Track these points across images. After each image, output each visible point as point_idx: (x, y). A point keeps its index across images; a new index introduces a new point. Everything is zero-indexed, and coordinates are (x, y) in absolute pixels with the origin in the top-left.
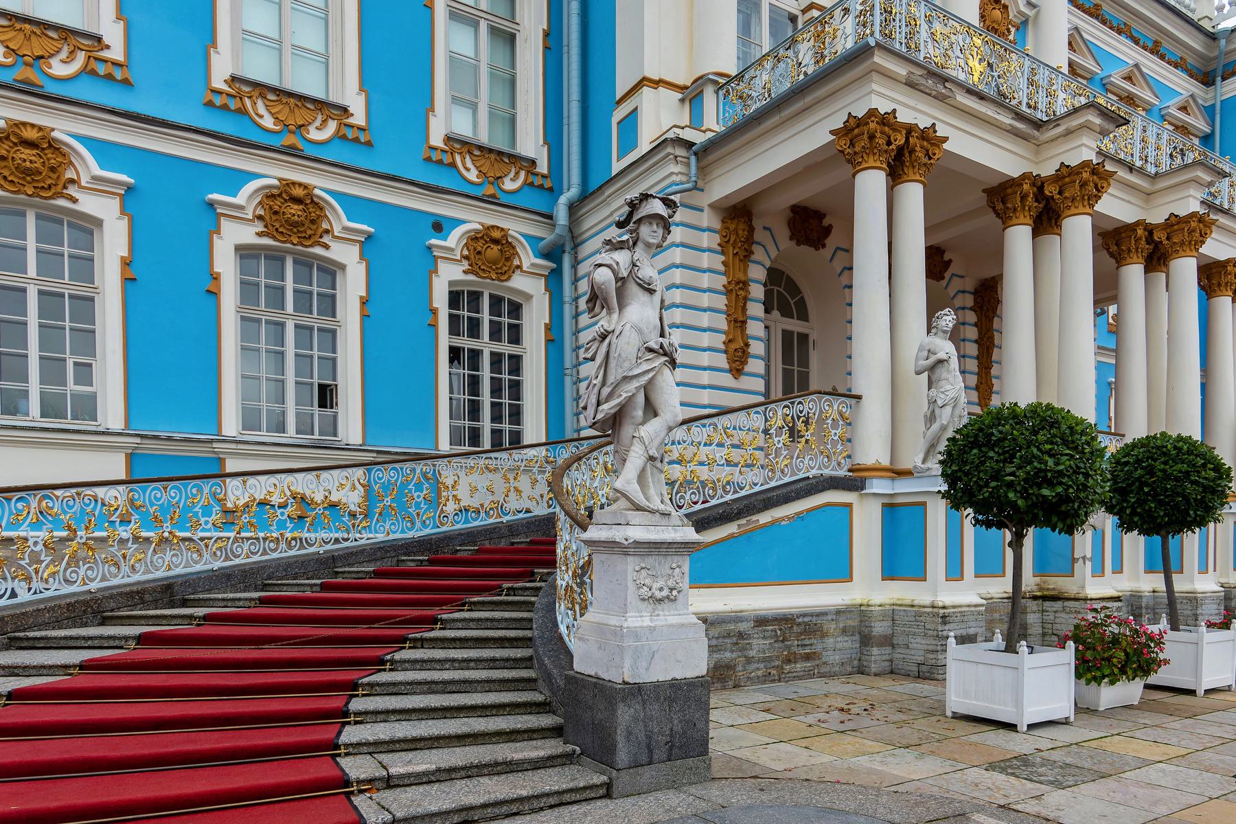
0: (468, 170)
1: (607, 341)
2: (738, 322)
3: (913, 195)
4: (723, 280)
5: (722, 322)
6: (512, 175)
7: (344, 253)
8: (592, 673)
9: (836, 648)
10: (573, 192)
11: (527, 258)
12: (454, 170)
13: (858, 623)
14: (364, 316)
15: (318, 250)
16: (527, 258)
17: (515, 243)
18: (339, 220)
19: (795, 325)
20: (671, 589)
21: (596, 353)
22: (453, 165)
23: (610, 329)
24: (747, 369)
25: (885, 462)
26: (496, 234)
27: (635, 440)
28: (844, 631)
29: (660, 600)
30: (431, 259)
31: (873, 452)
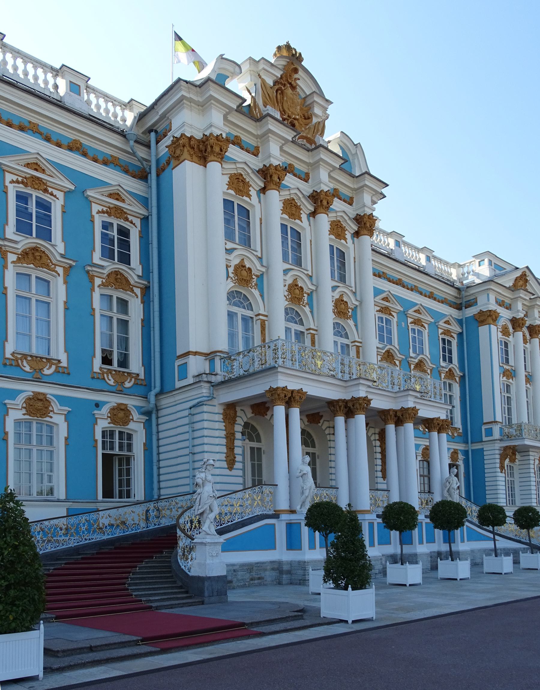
0: (110, 380)
2: (230, 448)
4: (224, 432)
5: (224, 449)
6: (128, 380)
10: (158, 389)
11: (135, 415)
16: (135, 415)
18: (56, 406)
19: (255, 445)
24: (235, 467)
31: (283, 505)
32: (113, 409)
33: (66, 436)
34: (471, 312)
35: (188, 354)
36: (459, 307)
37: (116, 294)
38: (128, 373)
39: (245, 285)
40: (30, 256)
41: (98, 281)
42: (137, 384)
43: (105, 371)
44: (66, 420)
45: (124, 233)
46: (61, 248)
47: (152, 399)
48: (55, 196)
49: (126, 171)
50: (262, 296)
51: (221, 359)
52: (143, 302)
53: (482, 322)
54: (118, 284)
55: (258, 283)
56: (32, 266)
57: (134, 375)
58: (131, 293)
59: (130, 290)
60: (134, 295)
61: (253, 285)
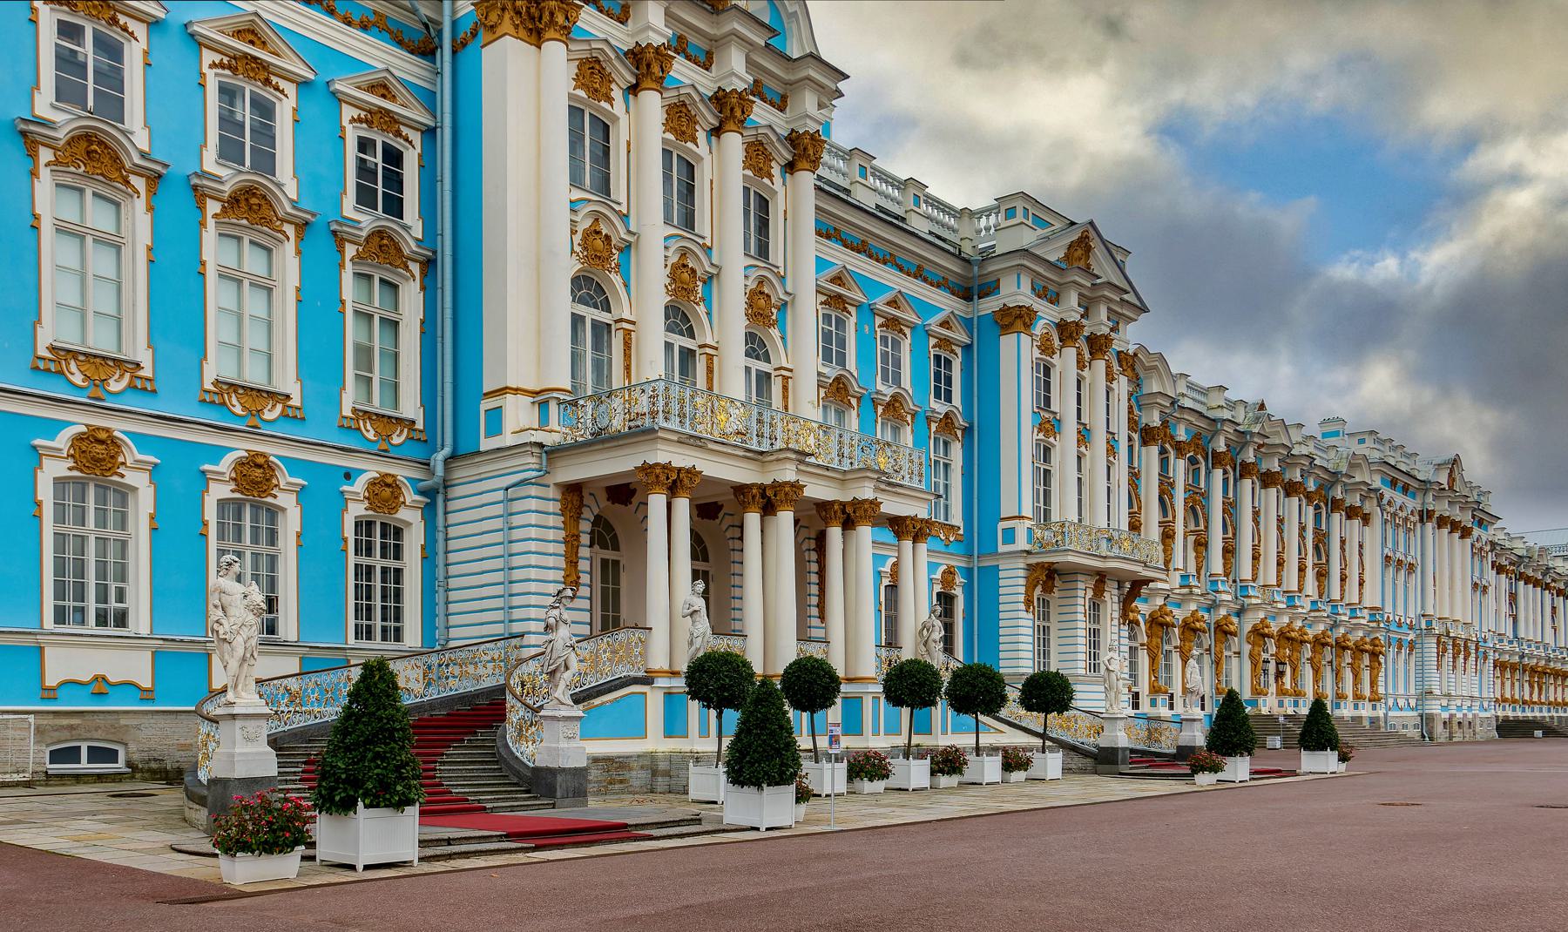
2: (572, 561)
5: (562, 562)
7: (285, 500)
9: (638, 777)
10: (447, 451)
11: (410, 496)
12: (357, 434)
13: (651, 764)
14: (299, 546)
15: (270, 500)
16: (410, 496)
18: (284, 478)
19: (610, 555)
25: (666, 668)
28: (642, 767)
30: (343, 498)
31: (659, 661)
32: (373, 483)
34: (989, 305)
35: (503, 391)
36: (966, 294)
40: (243, 204)
41: (350, 251)
45: (394, 157)
46: (291, 190)
48: (282, 92)
49: (400, 43)
52: (423, 288)
53: (1006, 328)
56: (244, 222)
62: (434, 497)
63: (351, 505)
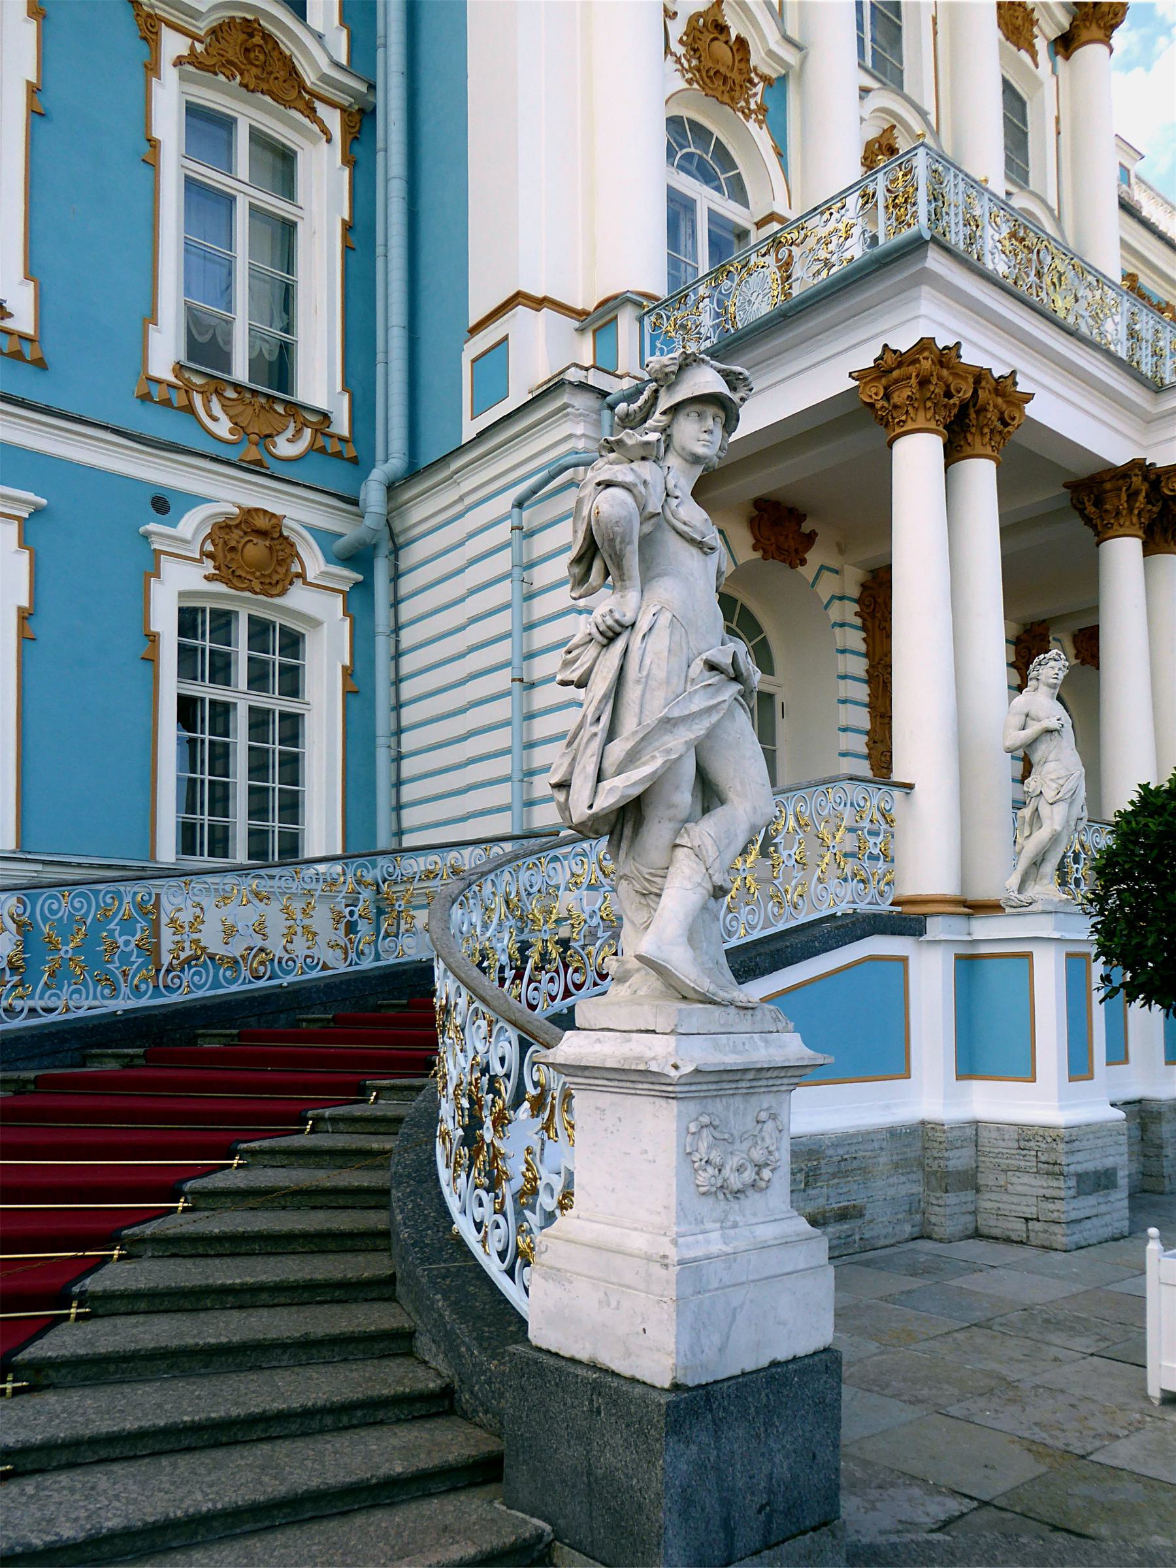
0: (215, 419)
1: (620, 644)
3: (981, 474)
6: (290, 433)
8: (583, 1356)
11: (314, 562)
17: (294, 538)
20: (759, 1167)
21: (590, 671)
22: (190, 409)
23: (627, 620)
26: (261, 523)
27: (680, 853)
29: (738, 1193)
33: (25, 603)
37: (250, 114)
38: (287, 403)
39: (726, 99)
41: (173, 45)
42: (322, 450)
43: (198, 380)
44: (23, 543)
47: (373, 494)
50: (781, 154)
51: (640, 320)
52: (349, 160)
54: (254, 71)
55: (770, 105)
57: (313, 418)
58: (306, 121)
59: (302, 106)
60: (315, 128)
61: (753, 106)
62: (369, 563)
63: (168, 566)
